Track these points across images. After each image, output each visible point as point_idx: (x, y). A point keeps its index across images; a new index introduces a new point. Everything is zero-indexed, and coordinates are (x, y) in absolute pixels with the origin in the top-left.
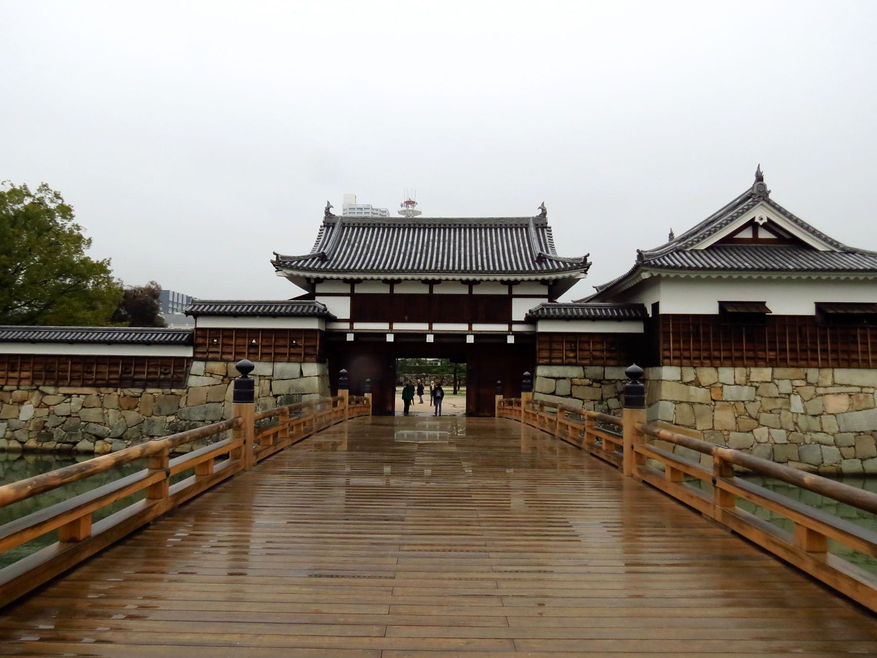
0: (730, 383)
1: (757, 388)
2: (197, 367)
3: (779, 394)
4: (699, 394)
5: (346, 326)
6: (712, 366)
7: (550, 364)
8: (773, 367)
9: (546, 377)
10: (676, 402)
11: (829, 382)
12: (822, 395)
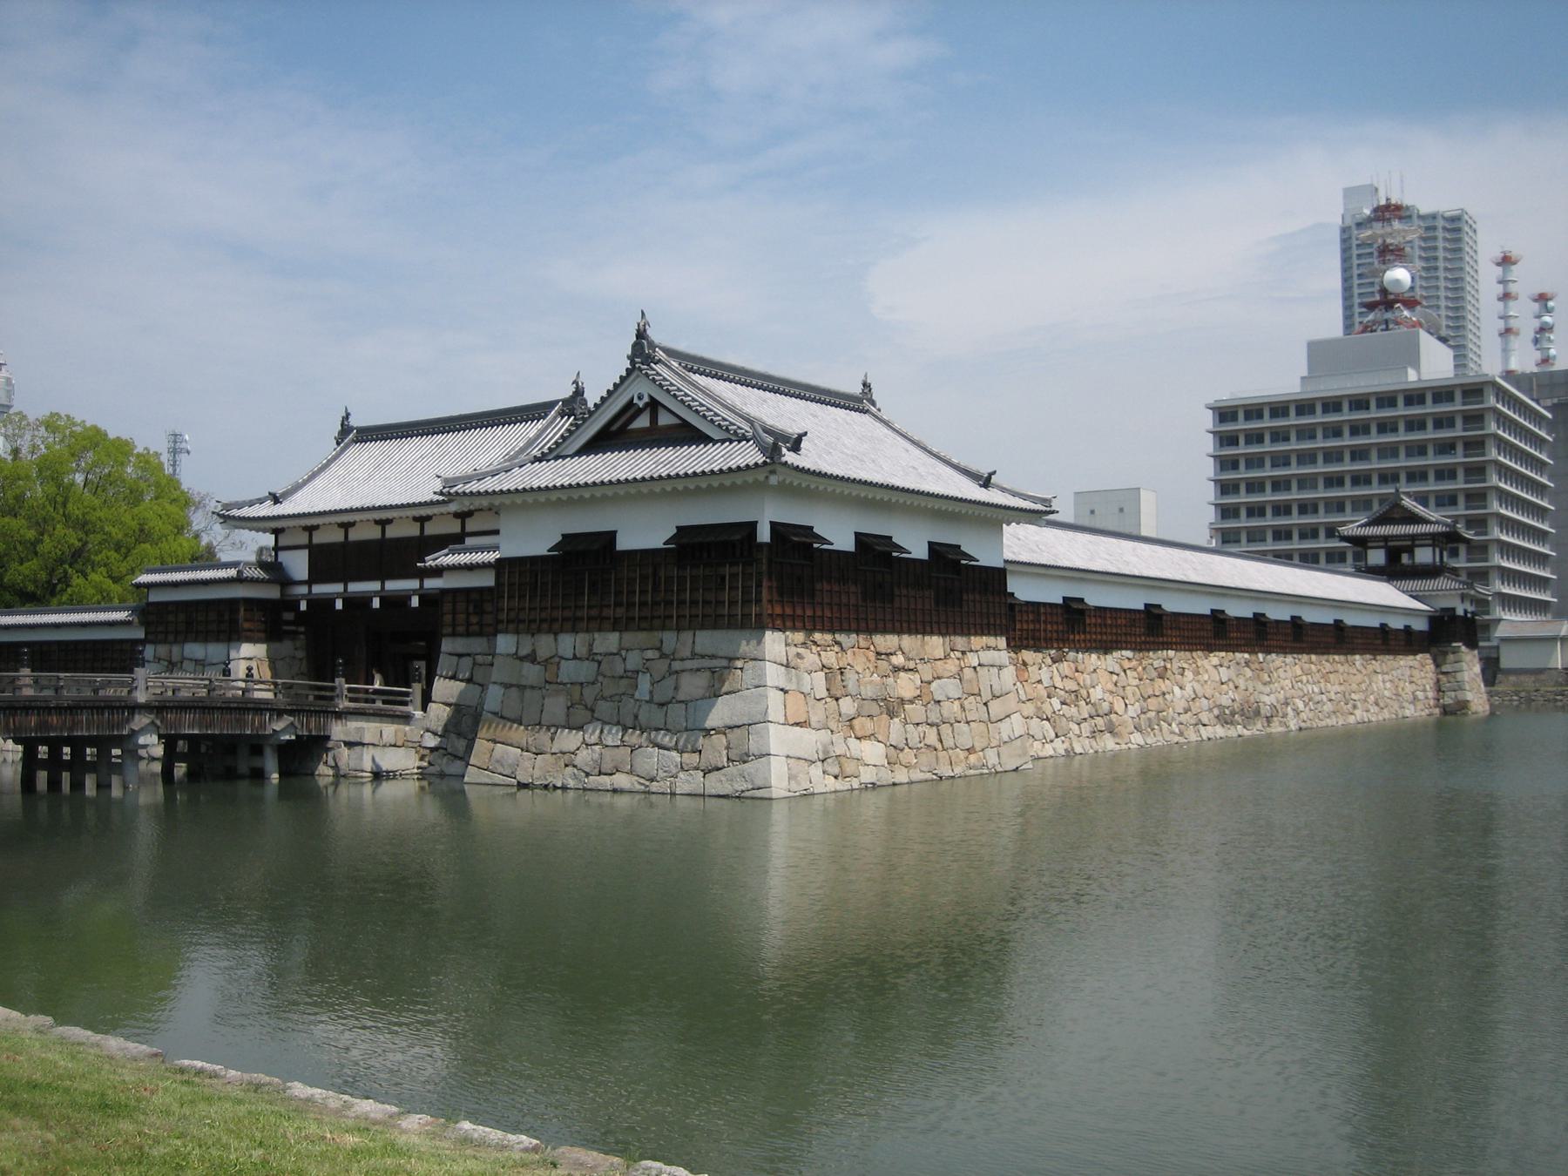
0: (567, 656)
1: (600, 663)
2: (149, 651)
3: (625, 671)
4: (532, 673)
5: (303, 590)
6: (549, 631)
7: (454, 634)
8: (620, 631)
9: (450, 654)
10: (507, 686)
11: (688, 653)
12: (677, 672)
